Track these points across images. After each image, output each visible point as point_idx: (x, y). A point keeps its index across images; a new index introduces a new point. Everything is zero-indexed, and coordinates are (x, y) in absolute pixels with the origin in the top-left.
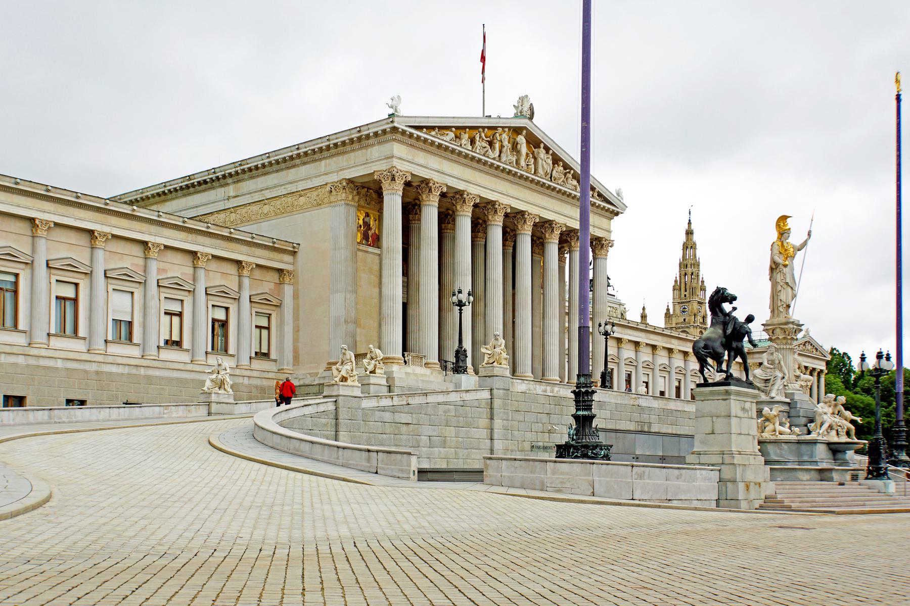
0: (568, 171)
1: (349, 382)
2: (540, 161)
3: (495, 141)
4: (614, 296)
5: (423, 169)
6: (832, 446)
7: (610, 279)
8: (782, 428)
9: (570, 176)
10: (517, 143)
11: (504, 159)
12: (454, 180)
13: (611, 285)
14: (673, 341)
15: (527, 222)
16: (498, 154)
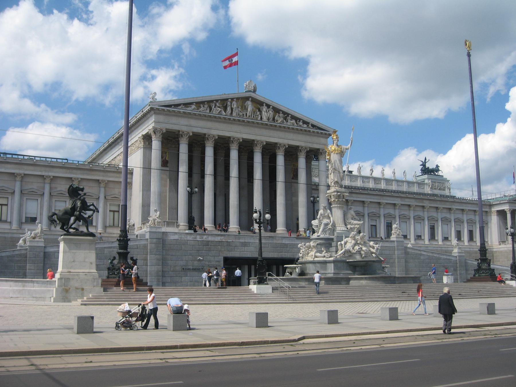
0: (286, 115)
1: (37, 239)
2: (263, 112)
3: (228, 106)
4: (443, 176)
5: (176, 126)
6: (350, 263)
7: (439, 167)
8: (318, 254)
9: (289, 118)
10: (245, 106)
11: (234, 114)
12: (199, 128)
13: (440, 170)
14: (425, 201)
15: (258, 145)
16: (230, 112)
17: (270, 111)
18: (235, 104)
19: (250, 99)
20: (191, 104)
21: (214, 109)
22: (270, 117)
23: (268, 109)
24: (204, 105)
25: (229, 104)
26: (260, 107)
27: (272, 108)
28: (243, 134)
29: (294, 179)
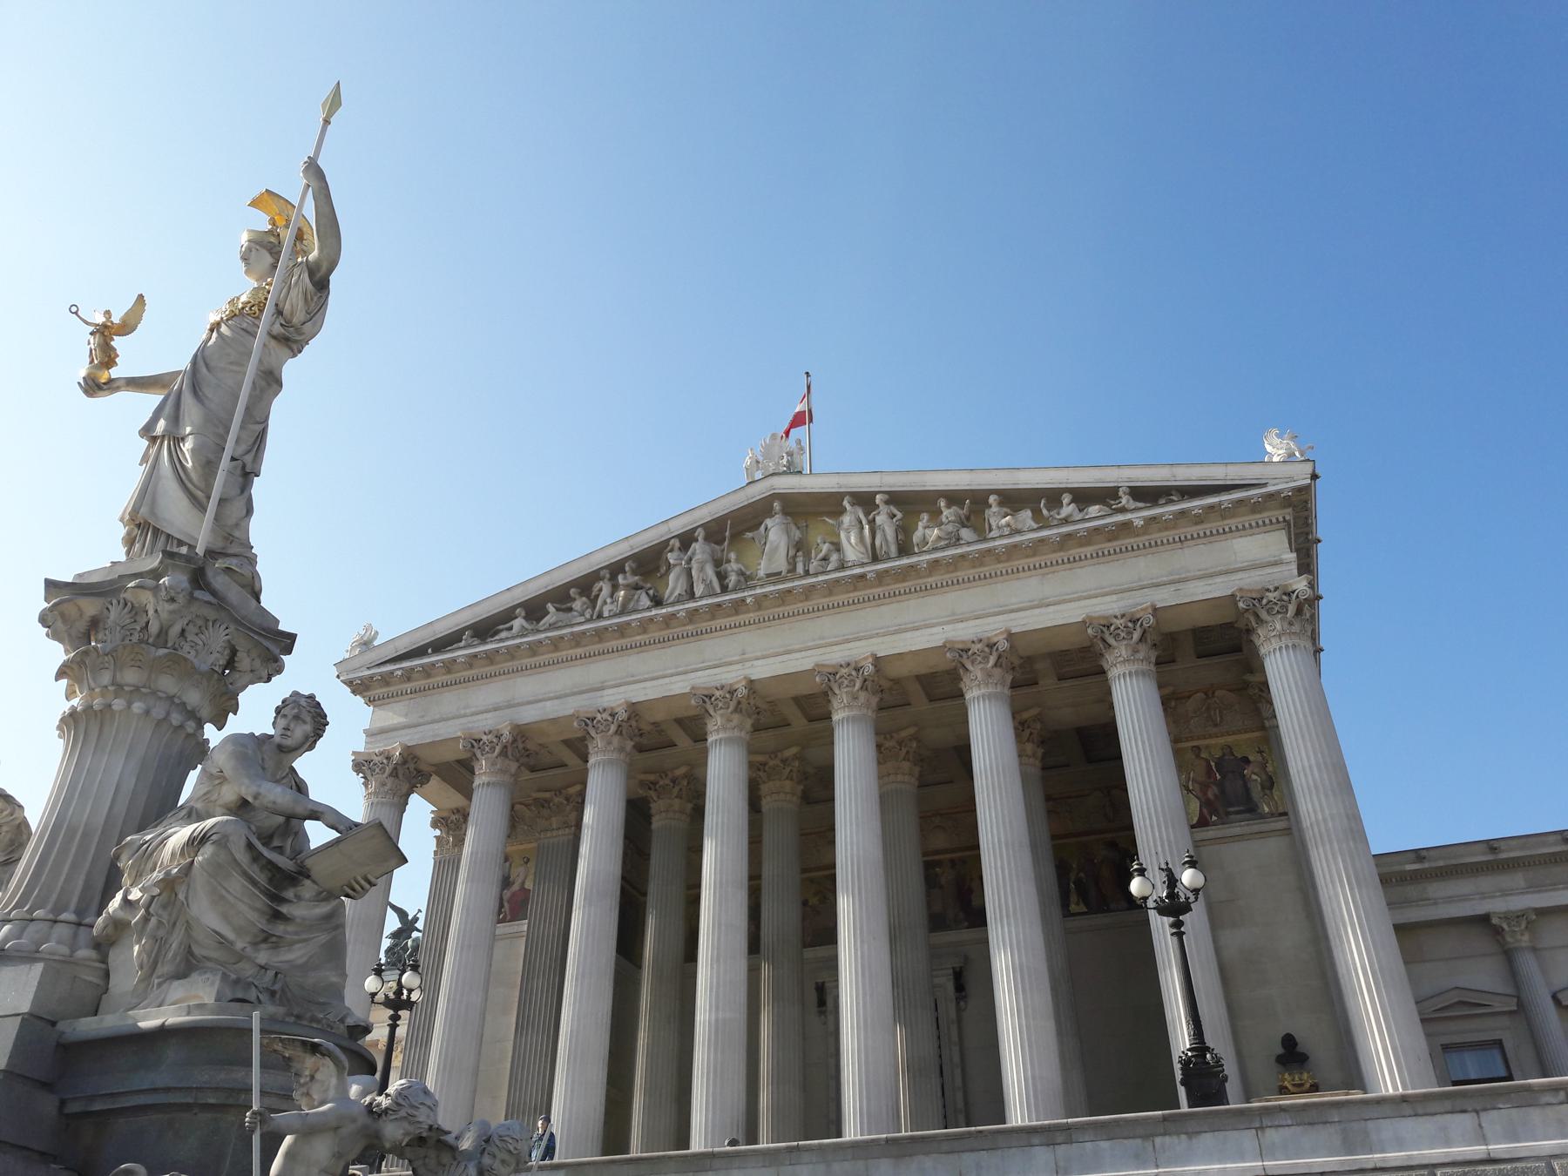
2: (843, 535)
5: (450, 723)
9: (995, 509)
11: (699, 589)
12: (548, 703)
17: (877, 518)
18: (698, 551)
19: (777, 505)
20: (507, 616)
21: (605, 603)
22: (878, 543)
23: (867, 514)
24: (569, 605)
25: (672, 561)
26: (830, 521)
27: (887, 503)
28: (755, 663)
29: (1214, 824)
